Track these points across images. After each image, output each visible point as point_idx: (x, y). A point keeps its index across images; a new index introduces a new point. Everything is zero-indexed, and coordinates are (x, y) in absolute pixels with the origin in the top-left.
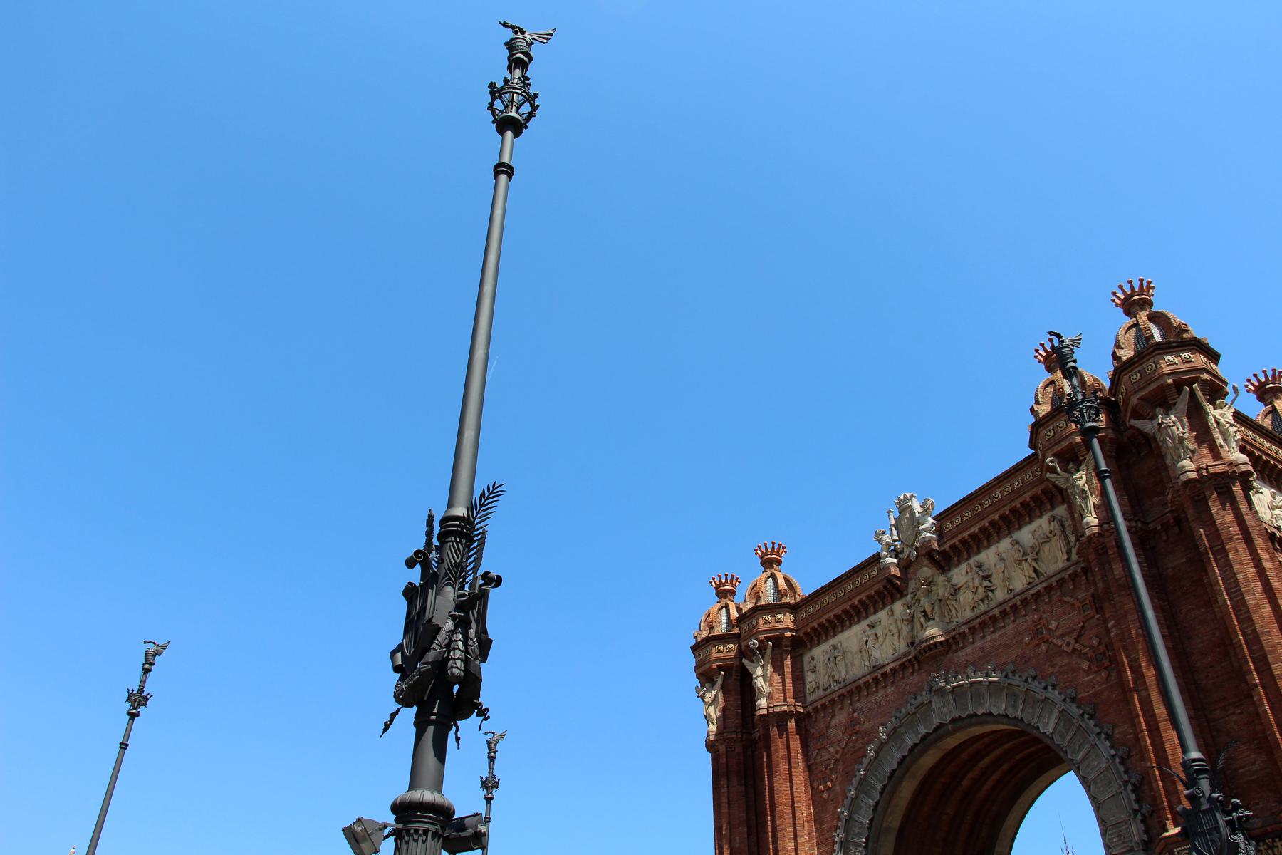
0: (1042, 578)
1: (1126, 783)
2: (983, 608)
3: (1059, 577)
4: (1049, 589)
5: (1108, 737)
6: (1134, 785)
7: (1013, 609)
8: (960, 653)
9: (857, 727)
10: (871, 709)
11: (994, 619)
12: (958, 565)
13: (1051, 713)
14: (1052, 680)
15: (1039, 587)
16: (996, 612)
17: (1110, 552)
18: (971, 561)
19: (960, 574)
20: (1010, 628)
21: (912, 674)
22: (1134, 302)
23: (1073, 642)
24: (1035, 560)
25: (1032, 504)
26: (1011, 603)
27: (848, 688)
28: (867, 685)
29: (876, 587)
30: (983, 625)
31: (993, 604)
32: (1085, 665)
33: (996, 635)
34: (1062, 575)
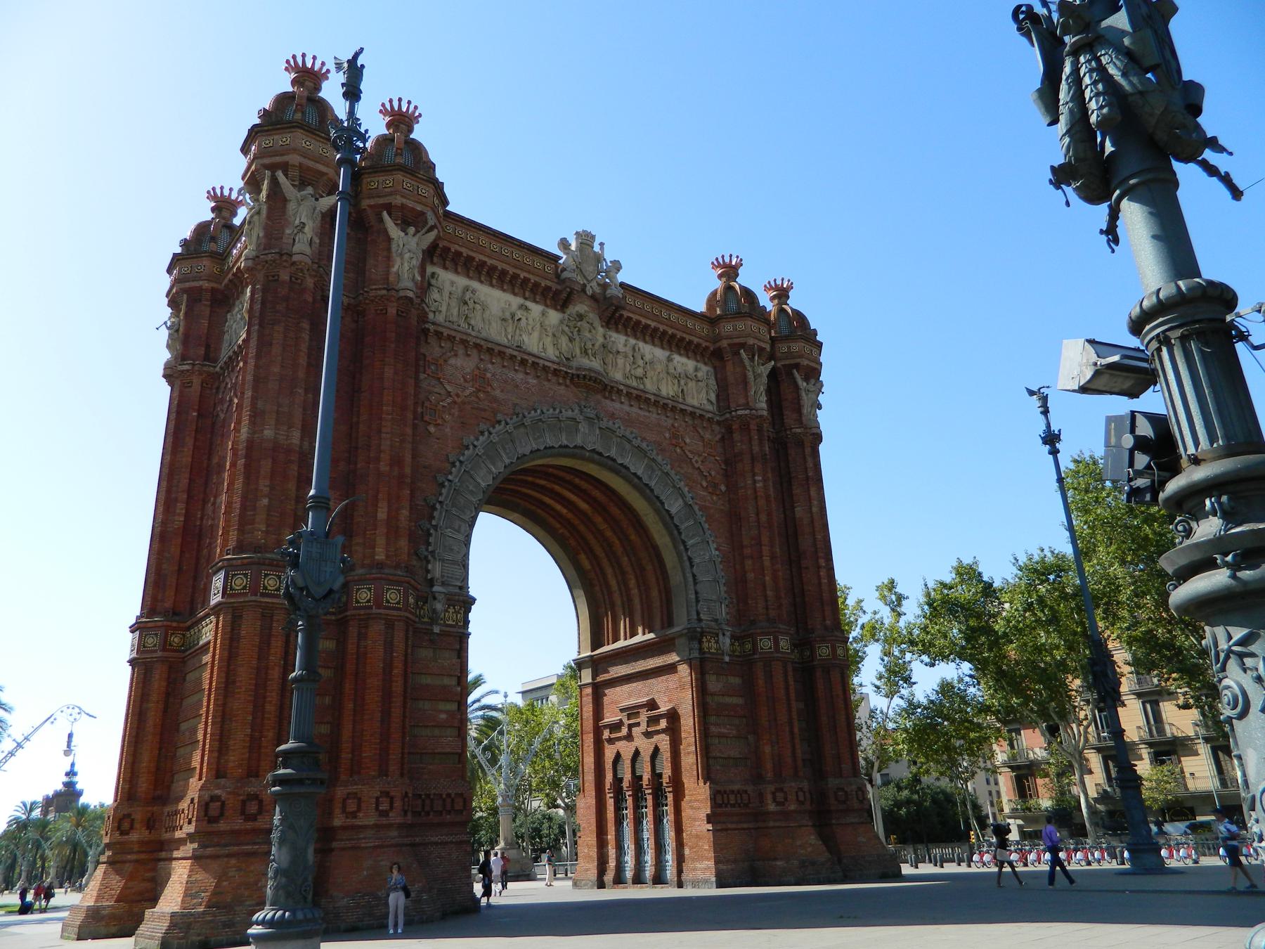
8: (608, 402)
9: (489, 389)
10: (506, 382)
11: (647, 400)
12: (617, 331)
18: (632, 341)
19: (620, 340)
20: (654, 416)
21: (560, 384)
27: (490, 345)
28: (512, 357)
29: (549, 283)
30: (638, 398)
31: (642, 387)
33: (642, 413)
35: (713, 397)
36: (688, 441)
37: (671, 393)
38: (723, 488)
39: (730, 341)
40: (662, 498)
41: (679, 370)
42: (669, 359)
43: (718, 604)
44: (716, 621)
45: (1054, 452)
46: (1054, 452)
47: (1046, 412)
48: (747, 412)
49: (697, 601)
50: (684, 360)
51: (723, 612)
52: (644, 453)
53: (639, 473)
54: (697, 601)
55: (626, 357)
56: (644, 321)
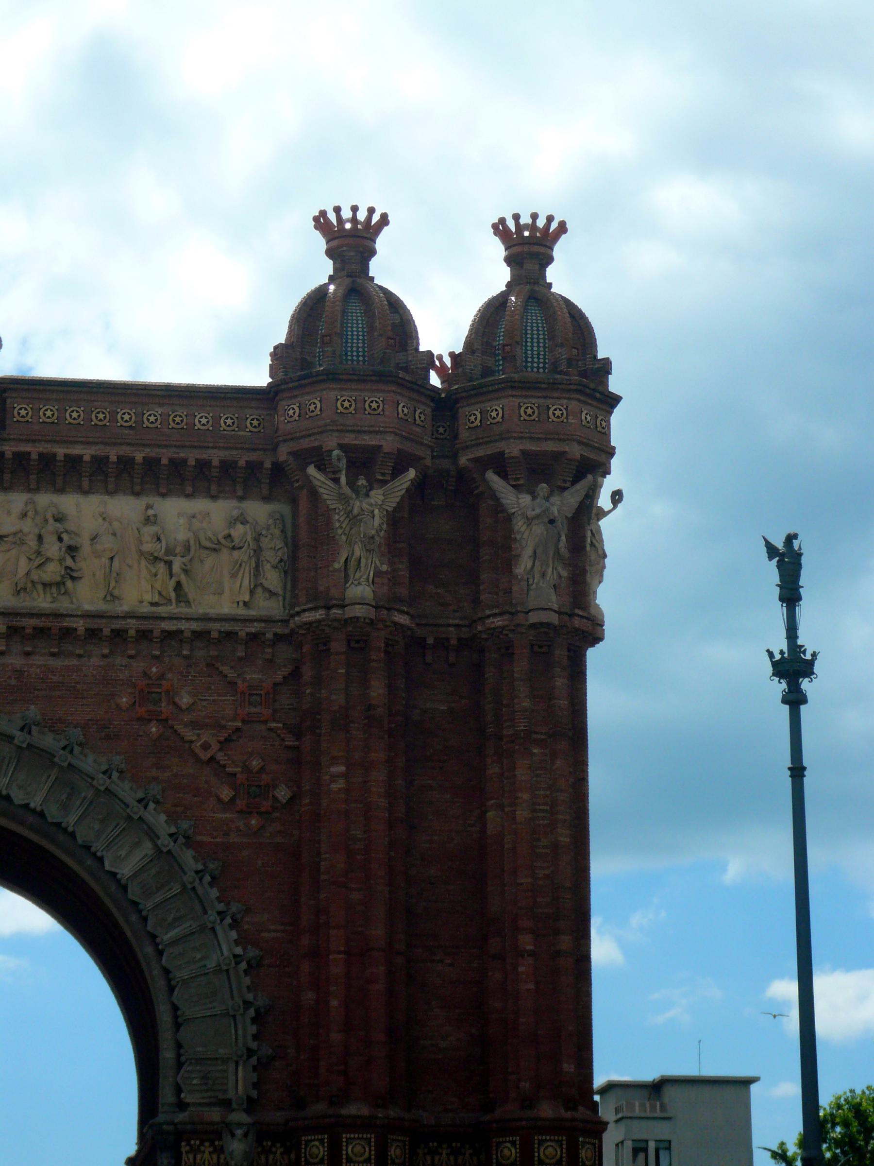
0: (183, 610)
1: (247, 1004)
2: (42, 602)
3: (227, 627)
4: (198, 635)
5: (235, 924)
6: (257, 1011)
7: (112, 634)
11: (67, 633)
13: (138, 844)
14: (155, 790)
15: (183, 626)
16: (80, 625)
17: (374, 656)
18: (44, 499)
22: (529, 247)
23: (215, 746)
24: (186, 571)
25: (215, 472)
26: (117, 625)
30: (41, 632)
31: (64, 605)
32: (226, 793)
33: (57, 663)
34: (236, 627)
35: (272, 578)
36: (185, 700)
37: (148, 597)
38: (283, 793)
39: (293, 446)
40: (98, 847)
41: (182, 535)
42: (148, 521)
43: (232, 1066)
44: (227, 1104)
45: (795, 700)
46: (795, 700)
47: (790, 595)
48: (319, 615)
49: (179, 1065)
50: (200, 505)
51: (239, 1082)
52: (46, 757)
53: (36, 803)
54: (179, 1065)
55: (22, 543)
56: (61, 451)
